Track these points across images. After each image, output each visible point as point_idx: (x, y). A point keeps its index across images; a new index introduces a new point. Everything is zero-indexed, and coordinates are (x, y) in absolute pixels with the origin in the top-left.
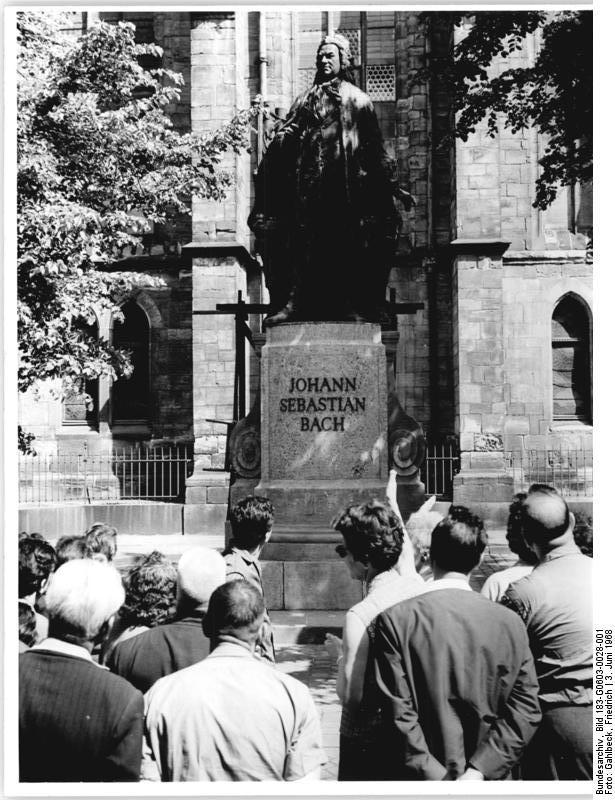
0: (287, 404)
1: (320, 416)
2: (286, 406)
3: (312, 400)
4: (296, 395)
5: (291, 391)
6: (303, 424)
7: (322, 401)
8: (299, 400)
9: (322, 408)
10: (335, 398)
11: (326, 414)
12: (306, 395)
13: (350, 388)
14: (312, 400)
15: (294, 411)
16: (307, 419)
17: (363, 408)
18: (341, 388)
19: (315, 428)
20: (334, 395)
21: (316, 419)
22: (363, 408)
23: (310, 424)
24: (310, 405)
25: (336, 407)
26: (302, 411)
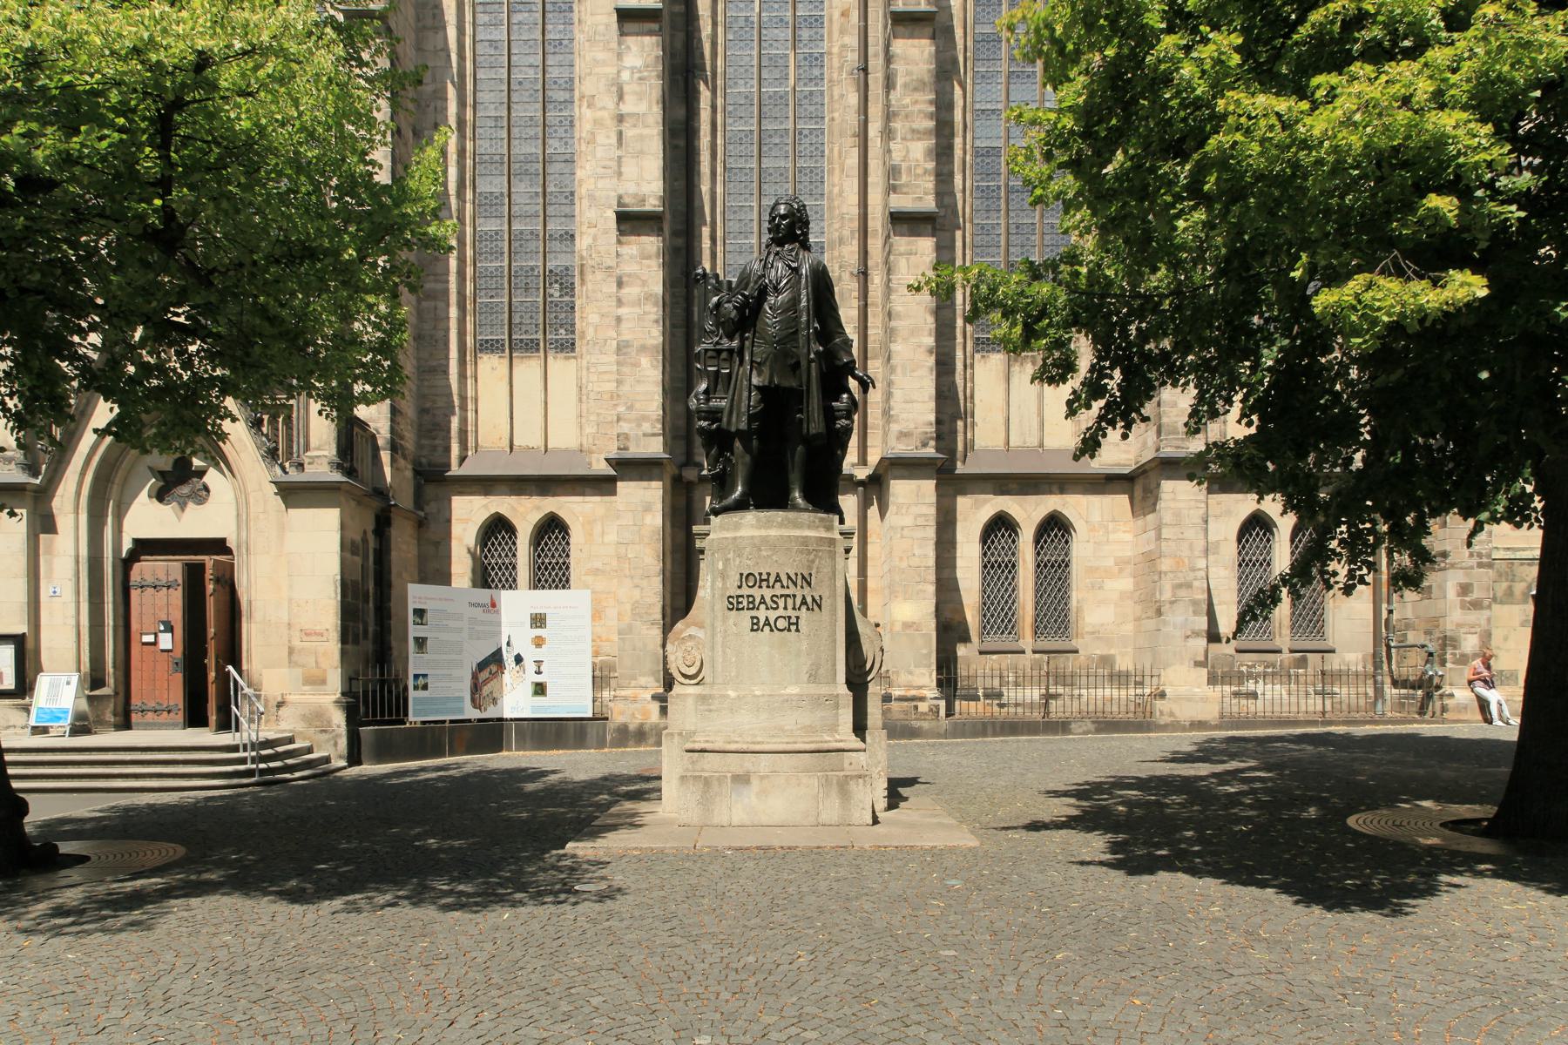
1: (772, 615)
2: (734, 604)
4: (745, 591)
17: (820, 607)
18: (795, 584)
19: (767, 628)
20: (786, 592)
22: (820, 607)
25: (790, 606)
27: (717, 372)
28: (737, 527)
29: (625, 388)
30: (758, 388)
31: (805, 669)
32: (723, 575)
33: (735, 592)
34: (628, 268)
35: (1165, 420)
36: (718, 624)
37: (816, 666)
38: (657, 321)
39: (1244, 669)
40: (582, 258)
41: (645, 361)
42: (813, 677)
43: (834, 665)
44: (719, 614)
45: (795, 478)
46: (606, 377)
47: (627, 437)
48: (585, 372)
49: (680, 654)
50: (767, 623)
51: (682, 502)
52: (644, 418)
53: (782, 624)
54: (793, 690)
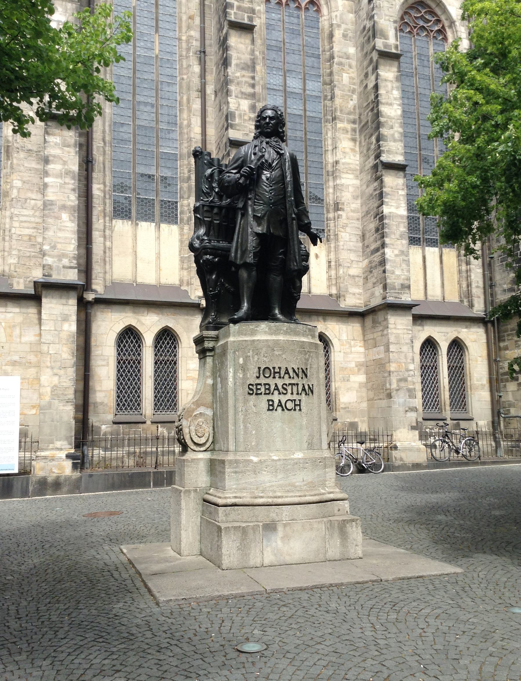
0: (254, 388)
2: (253, 390)
3: (276, 384)
4: (262, 380)
5: (258, 377)
6: (269, 405)
7: (285, 386)
8: (265, 384)
9: (285, 392)
10: (294, 384)
11: (289, 396)
12: (272, 382)
13: (304, 376)
14: (276, 385)
15: (261, 394)
16: (273, 401)
18: (298, 375)
19: (280, 409)
20: (293, 381)
21: (280, 401)
23: (276, 405)
24: (275, 389)
25: (295, 392)
26: (269, 394)
27: (211, 222)
28: (253, 333)
29: (50, 234)
30: (257, 234)
31: (305, 439)
32: (244, 368)
33: (253, 381)
34: (52, 151)
35: (388, 281)
36: (240, 405)
37: (311, 436)
38: (74, 190)
39: (428, 430)
40: (8, 141)
41: (65, 216)
42: (311, 446)
43: (320, 436)
44: (241, 398)
45: (275, 299)
46: (26, 225)
47: (50, 267)
48: (8, 220)
49: (193, 428)
50: (280, 404)
51: (83, 316)
52: (64, 255)
53: (290, 405)
54: (299, 455)
